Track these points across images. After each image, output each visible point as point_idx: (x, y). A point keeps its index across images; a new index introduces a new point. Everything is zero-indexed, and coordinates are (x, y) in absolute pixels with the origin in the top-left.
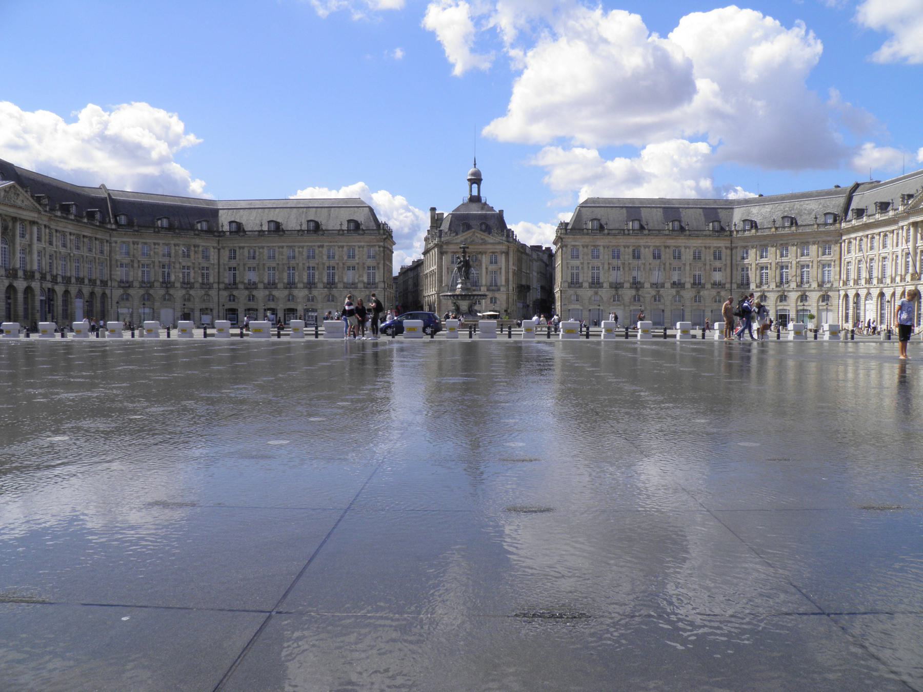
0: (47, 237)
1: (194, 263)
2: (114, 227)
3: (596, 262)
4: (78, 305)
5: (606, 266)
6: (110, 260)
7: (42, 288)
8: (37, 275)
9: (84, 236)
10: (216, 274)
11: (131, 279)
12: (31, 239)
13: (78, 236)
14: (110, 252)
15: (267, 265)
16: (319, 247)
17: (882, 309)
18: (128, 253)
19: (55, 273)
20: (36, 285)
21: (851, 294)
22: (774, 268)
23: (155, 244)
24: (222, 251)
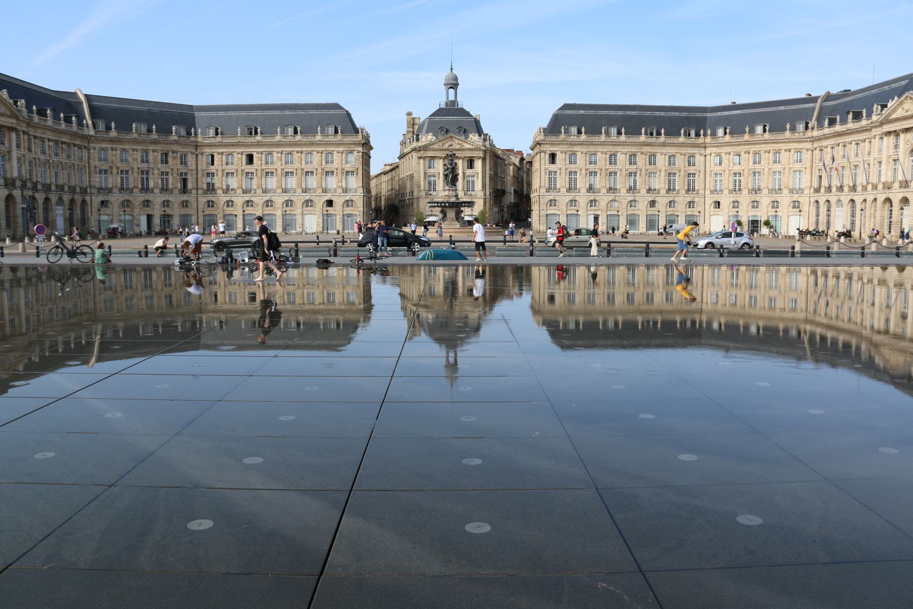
0: (26, 144)
1: (172, 170)
2: (92, 132)
3: (573, 167)
4: (59, 215)
5: (583, 172)
6: (89, 167)
7: (23, 196)
8: (18, 183)
9: (63, 143)
10: (195, 180)
11: (110, 186)
12: (10, 146)
13: (56, 142)
14: (89, 158)
15: (246, 171)
16: (298, 152)
17: (853, 216)
18: (106, 160)
19: (35, 180)
20: (17, 193)
21: (822, 200)
22: (746, 175)
23: (133, 150)
24: (200, 156)
